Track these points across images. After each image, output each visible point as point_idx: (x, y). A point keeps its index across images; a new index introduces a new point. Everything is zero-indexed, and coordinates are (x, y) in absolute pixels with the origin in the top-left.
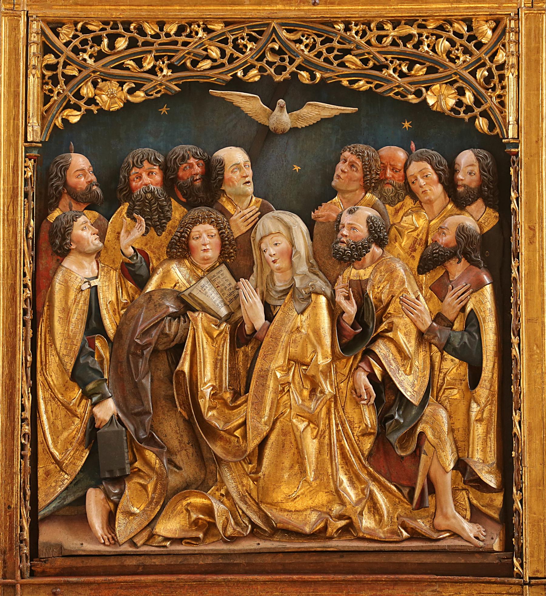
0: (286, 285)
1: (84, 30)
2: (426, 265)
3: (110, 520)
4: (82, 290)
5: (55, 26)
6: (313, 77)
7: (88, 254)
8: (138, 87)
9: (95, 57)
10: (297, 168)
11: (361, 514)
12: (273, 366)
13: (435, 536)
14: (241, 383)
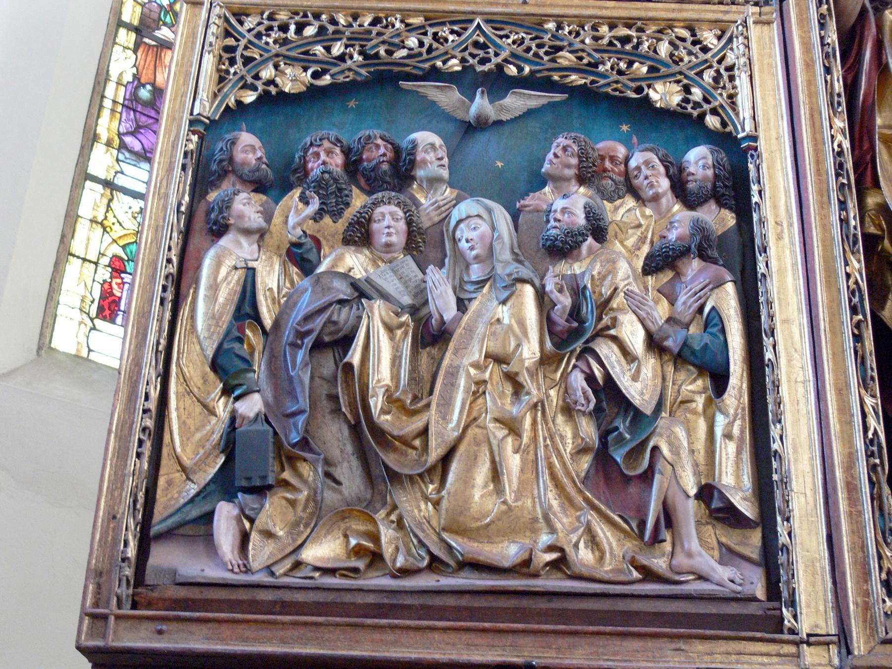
2: (652, 262)
5: (240, 15)
6: (520, 69)
7: (247, 232)
8: (324, 72)
10: (500, 164)
11: (576, 546)
12: (466, 362)
13: (677, 578)
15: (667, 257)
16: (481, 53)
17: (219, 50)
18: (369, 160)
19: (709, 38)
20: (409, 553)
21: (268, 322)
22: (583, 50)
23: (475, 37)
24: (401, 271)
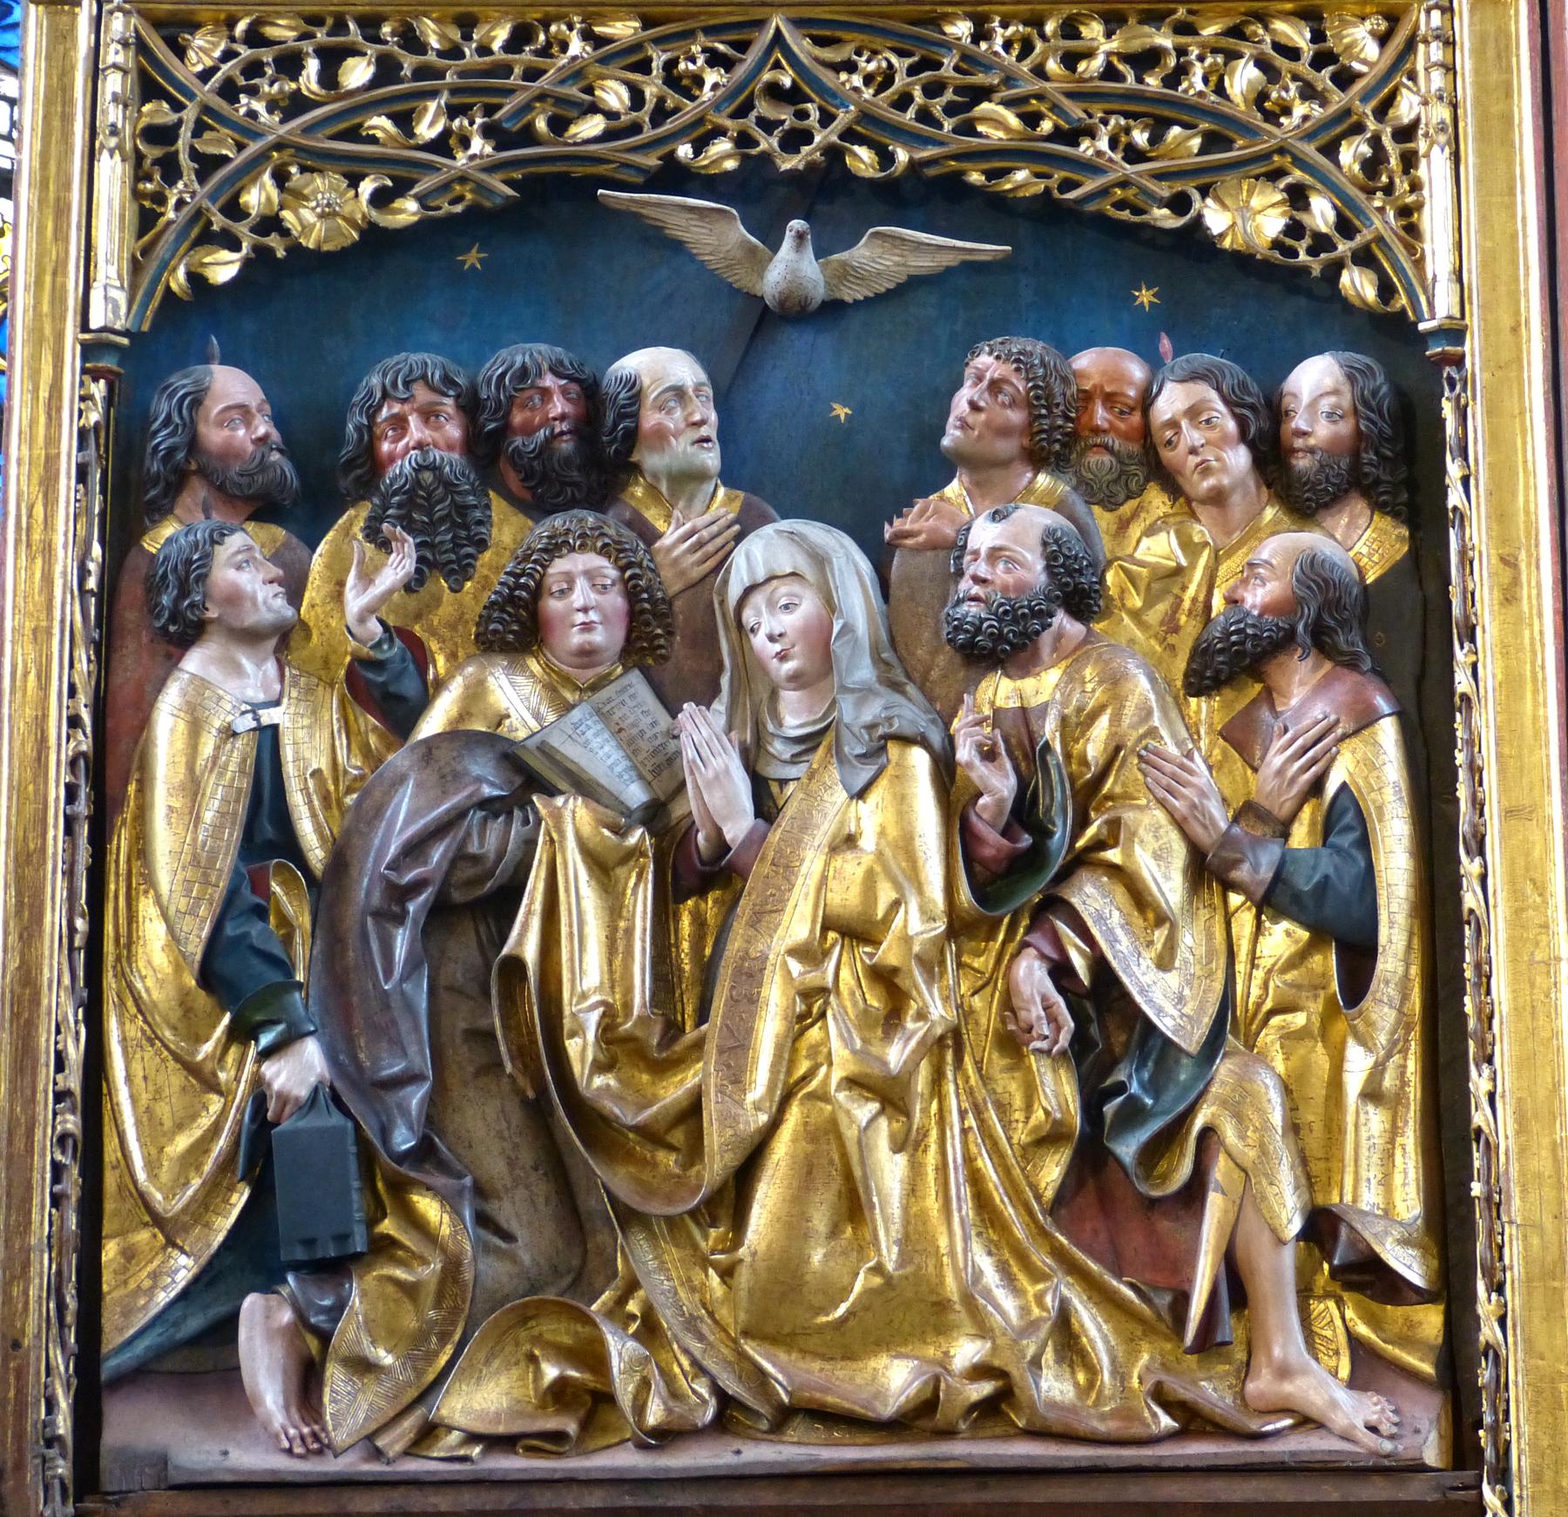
0: (815, 722)
1: (255, 38)
2: (1207, 668)
3: (307, 1384)
4: (235, 734)
6: (886, 158)
7: (250, 637)
8: (401, 187)
9: (283, 110)
10: (842, 412)
11: (1036, 1363)
13: (1254, 1425)
14: (685, 1001)
15: (1241, 654)
16: (786, 116)
17: (134, 137)
18: (529, 430)
19: (1361, 42)
20: (674, 1394)
21: (316, 854)
22: (1040, 97)
23: (767, 76)
24: (618, 714)
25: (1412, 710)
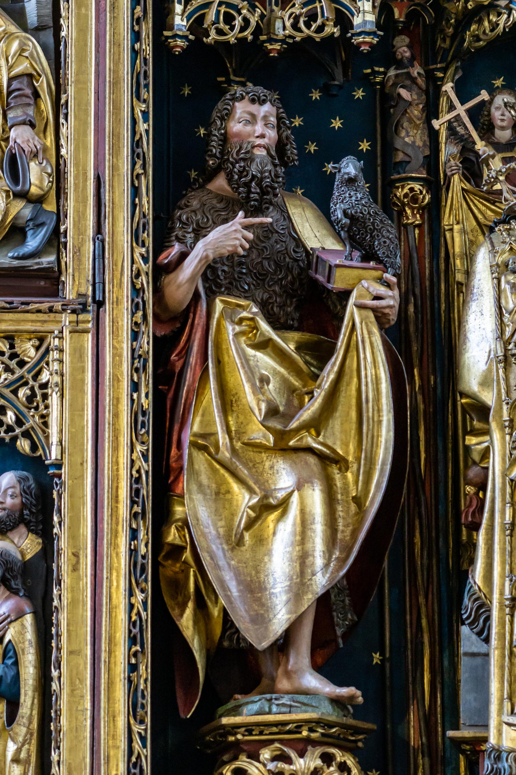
19: (28, 350)
25: (40, 610)
